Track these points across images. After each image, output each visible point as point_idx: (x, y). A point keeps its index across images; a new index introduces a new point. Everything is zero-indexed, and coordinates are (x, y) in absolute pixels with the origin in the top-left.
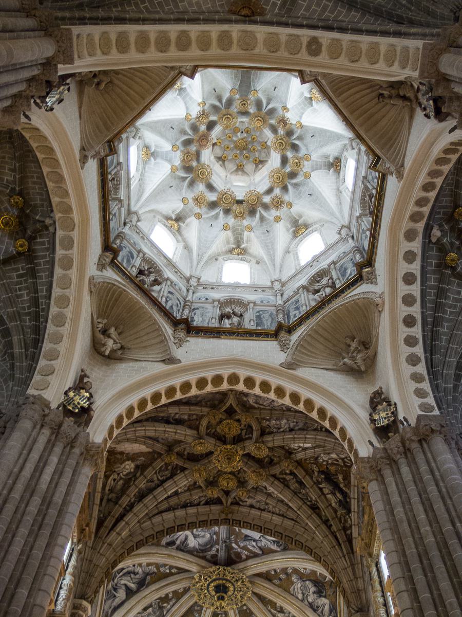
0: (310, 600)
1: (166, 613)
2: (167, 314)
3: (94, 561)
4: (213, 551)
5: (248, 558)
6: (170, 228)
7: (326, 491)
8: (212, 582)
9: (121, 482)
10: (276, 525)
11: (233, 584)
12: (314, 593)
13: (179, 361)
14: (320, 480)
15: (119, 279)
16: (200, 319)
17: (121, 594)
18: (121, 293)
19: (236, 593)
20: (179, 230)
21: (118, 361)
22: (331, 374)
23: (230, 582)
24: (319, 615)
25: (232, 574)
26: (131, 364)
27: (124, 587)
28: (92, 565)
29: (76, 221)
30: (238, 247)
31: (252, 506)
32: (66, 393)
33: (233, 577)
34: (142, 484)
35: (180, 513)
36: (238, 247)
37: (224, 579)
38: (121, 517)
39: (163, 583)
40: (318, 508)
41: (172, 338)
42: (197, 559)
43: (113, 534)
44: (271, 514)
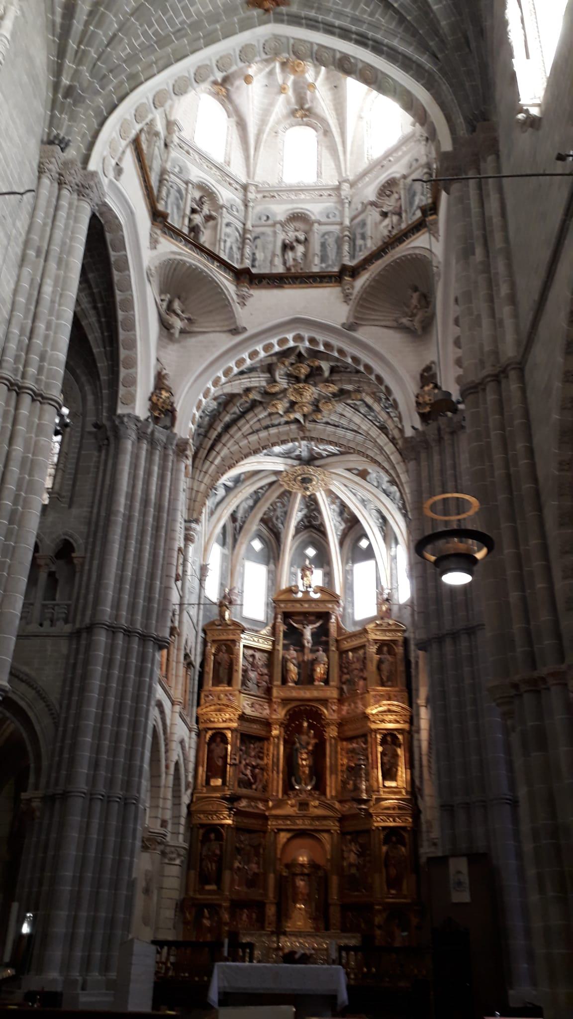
0: (384, 487)
2: (225, 265)
3: (195, 488)
4: (297, 453)
5: (328, 456)
6: (216, 95)
7: (392, 415)
8: (298, 476)
9: (207, 419)
12: (388, 482)
13: (245, 329)
14: (387, 405)
15: (175, 249)
16: (262, 254)
17: (221, 492)
18: (179, 263)
20: (228, 97)
21: (188, 335)
22: (390, 333)
26: (201, 338)
27: (223, 486)
28: (194, 492)
29: (122, 221)
30: (302, 108)
31: (327, 423)
32: (150, 399)
34: (227, 418)
35: (263, 434)
36: (302, 108)
38: (212, 448)
39: (255, 478)
40: (386, 428)
41: (235, 297)
42: (282, 459)
43: (208, 463)
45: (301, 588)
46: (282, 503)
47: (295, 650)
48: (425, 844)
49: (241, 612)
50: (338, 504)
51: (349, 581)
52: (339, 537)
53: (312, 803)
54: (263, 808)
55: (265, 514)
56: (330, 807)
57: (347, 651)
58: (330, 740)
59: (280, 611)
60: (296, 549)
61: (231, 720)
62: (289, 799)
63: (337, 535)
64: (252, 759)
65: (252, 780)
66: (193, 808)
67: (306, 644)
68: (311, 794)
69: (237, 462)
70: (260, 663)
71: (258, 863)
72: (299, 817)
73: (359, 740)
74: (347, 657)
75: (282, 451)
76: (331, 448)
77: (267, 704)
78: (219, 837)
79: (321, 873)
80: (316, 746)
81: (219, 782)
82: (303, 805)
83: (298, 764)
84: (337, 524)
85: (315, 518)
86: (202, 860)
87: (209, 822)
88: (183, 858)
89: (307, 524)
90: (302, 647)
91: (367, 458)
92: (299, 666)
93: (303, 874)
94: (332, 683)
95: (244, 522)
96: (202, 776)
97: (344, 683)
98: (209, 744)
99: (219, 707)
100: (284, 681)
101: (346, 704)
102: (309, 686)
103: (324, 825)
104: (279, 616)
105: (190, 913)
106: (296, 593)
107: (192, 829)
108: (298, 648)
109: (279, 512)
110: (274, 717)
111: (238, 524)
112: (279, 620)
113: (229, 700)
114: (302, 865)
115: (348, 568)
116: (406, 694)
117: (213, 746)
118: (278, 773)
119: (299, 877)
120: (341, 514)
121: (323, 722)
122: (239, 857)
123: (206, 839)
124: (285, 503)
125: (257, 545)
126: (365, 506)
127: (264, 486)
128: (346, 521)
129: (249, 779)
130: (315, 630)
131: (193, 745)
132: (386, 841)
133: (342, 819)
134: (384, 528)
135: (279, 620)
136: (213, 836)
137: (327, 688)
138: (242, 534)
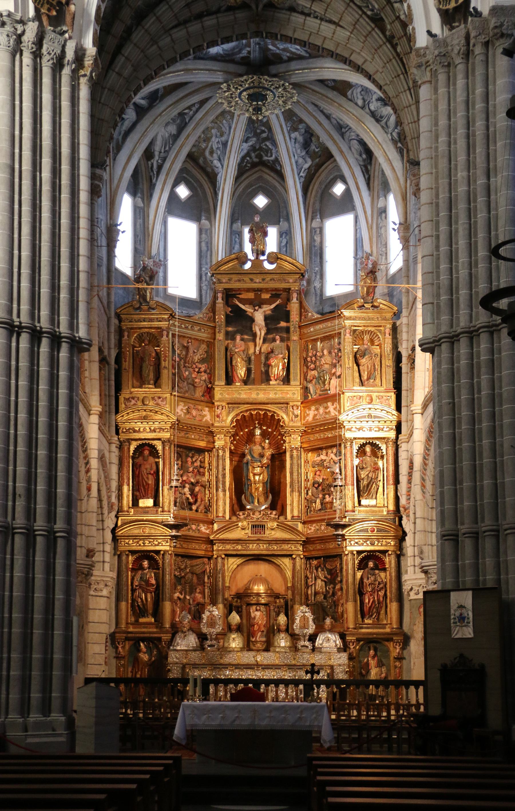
1: (189, 121)
10: (325, 38)
11: (272, 91)
19: (277, 98)
23: (268, 89)
24: (382, 127)
25: (270, 82)
33: (272, 85)
37: (261, 87)
44: (319, 22)
45: (251, 256)
46: (219, 129)
47: (242, 339)
48: (410, 570)
49: (165, 290)
50: (303, 131)
51: (317, 243)
52: (302, 180)
53: (270, 525)
54: (207, 532)
55: (194, 146)
56: (292, 530)
57: (316, 340)
58: (291, 451)
59: (220, 287)
60: (240, 197)
61: (161, 429)
62: (240, 520)
63: (300, 177)
64: (190, 475)
65: (191, 500)
66: (120, 533)
67: (258, 333)
68: (266, 515)
69: (156, 74)
70: (196, 358)
71: (203, 593)
72: (252, 541)
73: (330, 451)
74: (315, 348)
75: (221, 52)
76: (295, 48)
77: (207, 409)
78: (154, 565)
79: (280, 602)
80: (273, 457)
81: (150, 502)
82: (258, 527)
83: (249, 480)
84: (301, 160)
85: (268, 151)
86: (133, 591)
87: (139, 548)
88: (109, 589)
89: (256, 160)
90: (254, 335)
91: (345, 63)
92: (249, 361)
93: (258, 604)
94: (292, 383)
95: (164, 159)
96: (128, 496)
97: (311, 381)
98: (133, 458)
99: (144, 413)
100: (229, 380)
101: (313, 408)
102: (263, 386)
103: (283, 550)
104: (220, 295)
105: (123, 647)
106: (245, 263)
107: (119, 556)
108: (246, 337)
109: (214, 143)
110: (216, 424)
111: (155, 162)
112: (220, 300)
113: (158, 404)
114: (258, 595)
115: (315, 224)
116: (393, 396)
117: (140, 460)
118: (224, 491)
119: (254, 607)
120: (306, 145)
121: (282, 431)
122: (179, 587)
123: (137, 567)
124: (223, 129)
125: (183, 192)
126: (342, 135)
127: (193, 105)
128: (312, 155)
129: (188, 498)
130: (269, 312)
131: (115, 460)
132: (362, 565)
133: (307, 542)
134: (369, 167)
135: (220, 300)
136: (146, 563)
137: (286, 388)
138: (162, 177)
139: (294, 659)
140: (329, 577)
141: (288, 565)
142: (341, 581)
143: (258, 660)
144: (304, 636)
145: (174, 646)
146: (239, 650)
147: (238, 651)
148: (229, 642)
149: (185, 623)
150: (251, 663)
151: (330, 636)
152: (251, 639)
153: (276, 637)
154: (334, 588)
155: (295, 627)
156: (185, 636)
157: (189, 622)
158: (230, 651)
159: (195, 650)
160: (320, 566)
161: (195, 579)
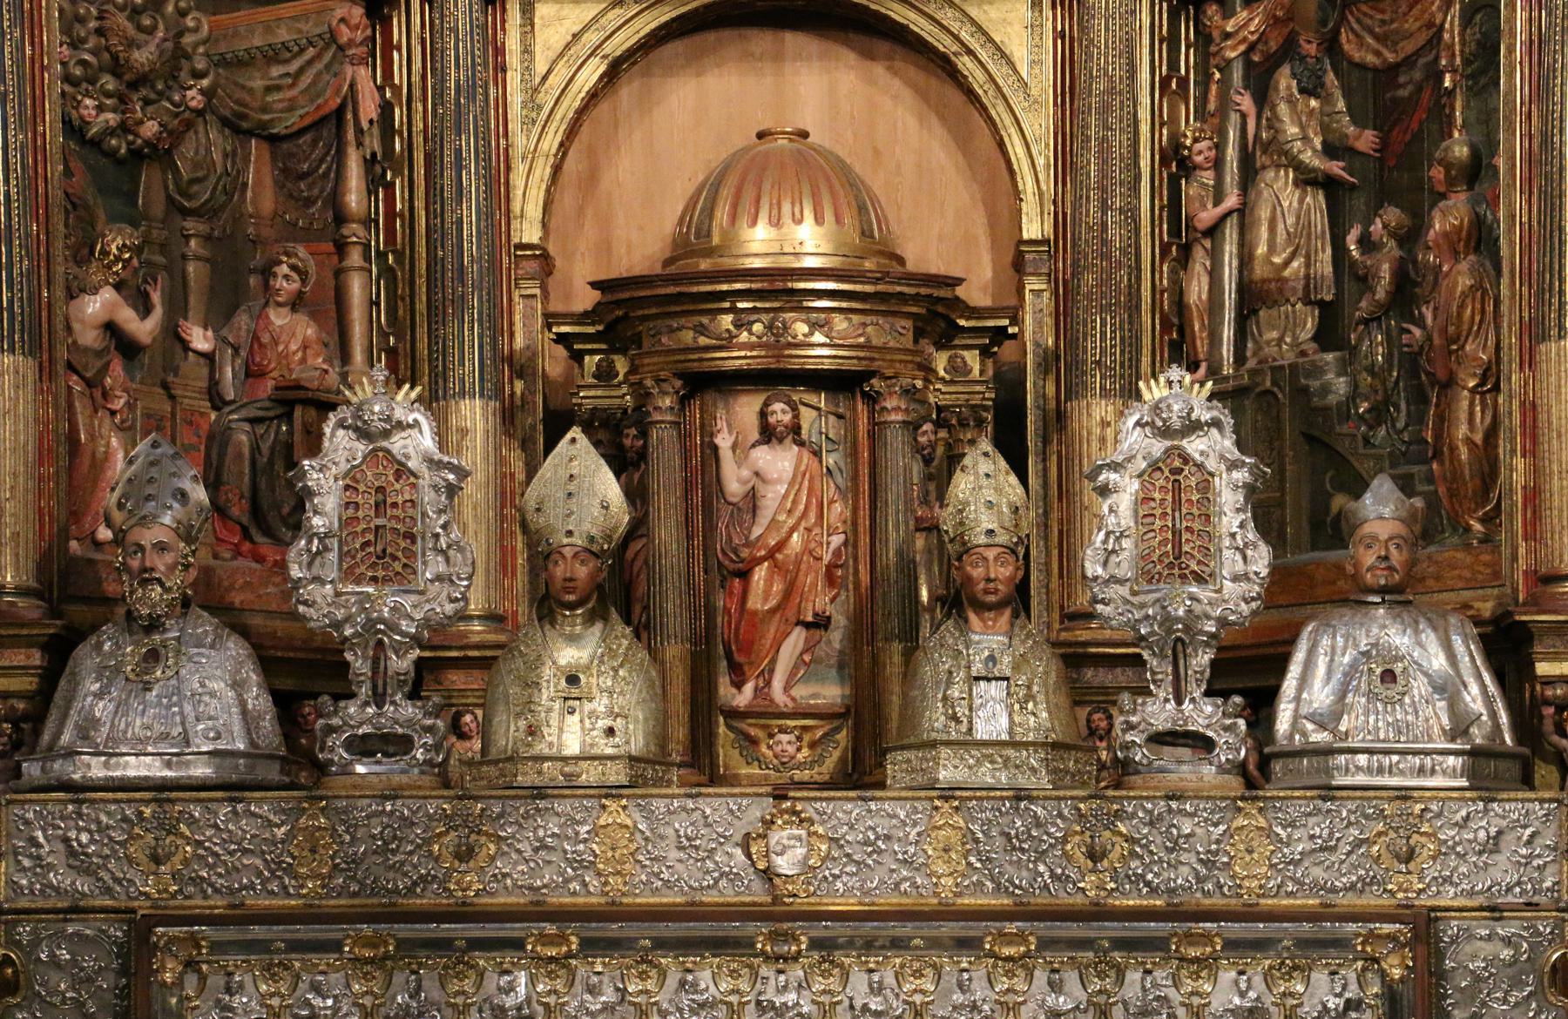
119: (747, 408)
122: (115, 241)
139: (1094, 855)
140: (1366, 140)
141: (1020, 51)
142: (1477, 171)
143: (784, 864)
144: (1178, 651)
145: (52, 752)
146: (617, 774)
147: (609, 791)
148: (528, 705)
149: (148, 537)
150: (727, 894)
151: (1398, 638)
152: (725, 690)
153: (936, 663)
154: (1410, 237)
155: (1093, 568)
156: (153, 656)
157: (186, 533)
158: (539, 792)
159: (232, 789)
160: (1288, 51)
161: (258, 171)
